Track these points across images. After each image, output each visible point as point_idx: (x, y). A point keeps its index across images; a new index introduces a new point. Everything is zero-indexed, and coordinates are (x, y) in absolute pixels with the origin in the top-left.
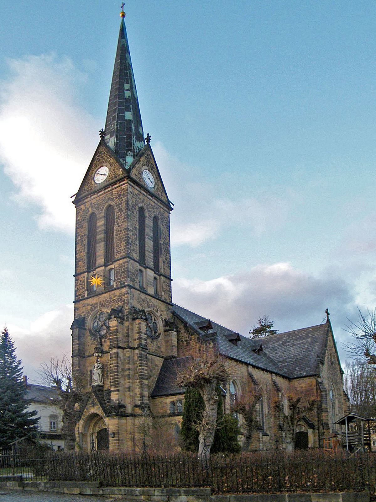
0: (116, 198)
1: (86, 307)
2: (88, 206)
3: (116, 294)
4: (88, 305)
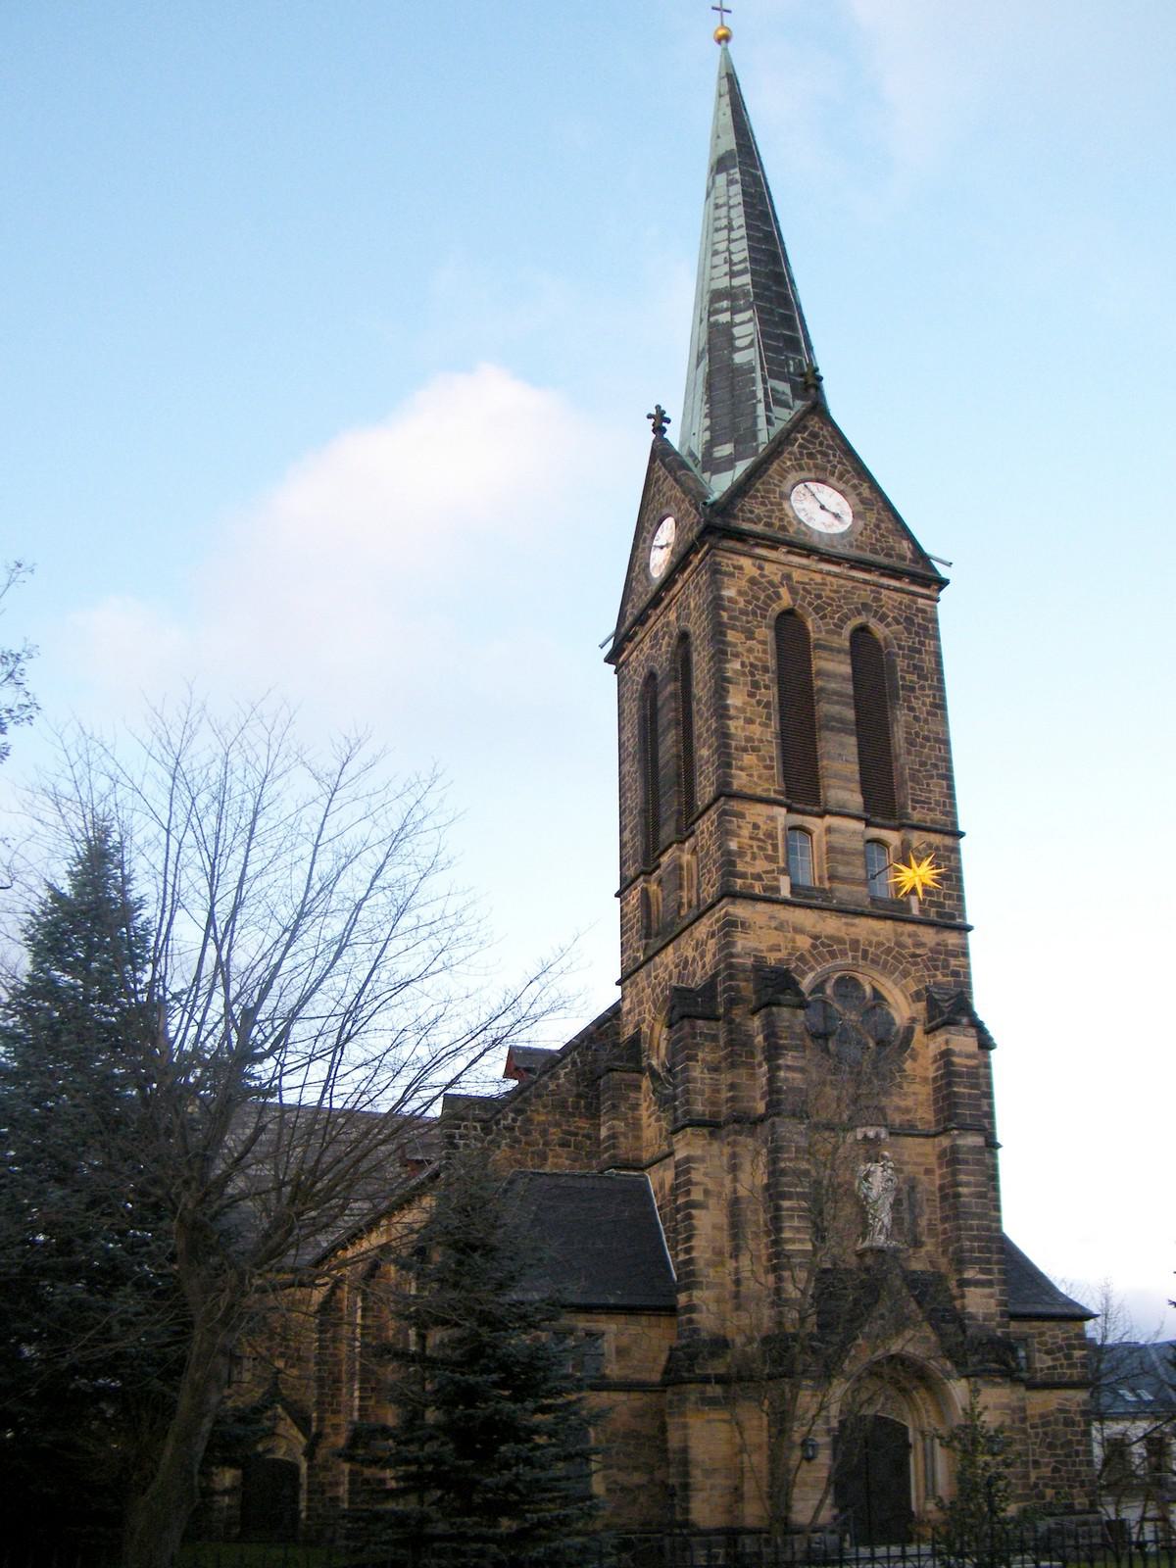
0: (898, 623)
1: (789, 935)
2: (777, 579)
3: (924, 940)
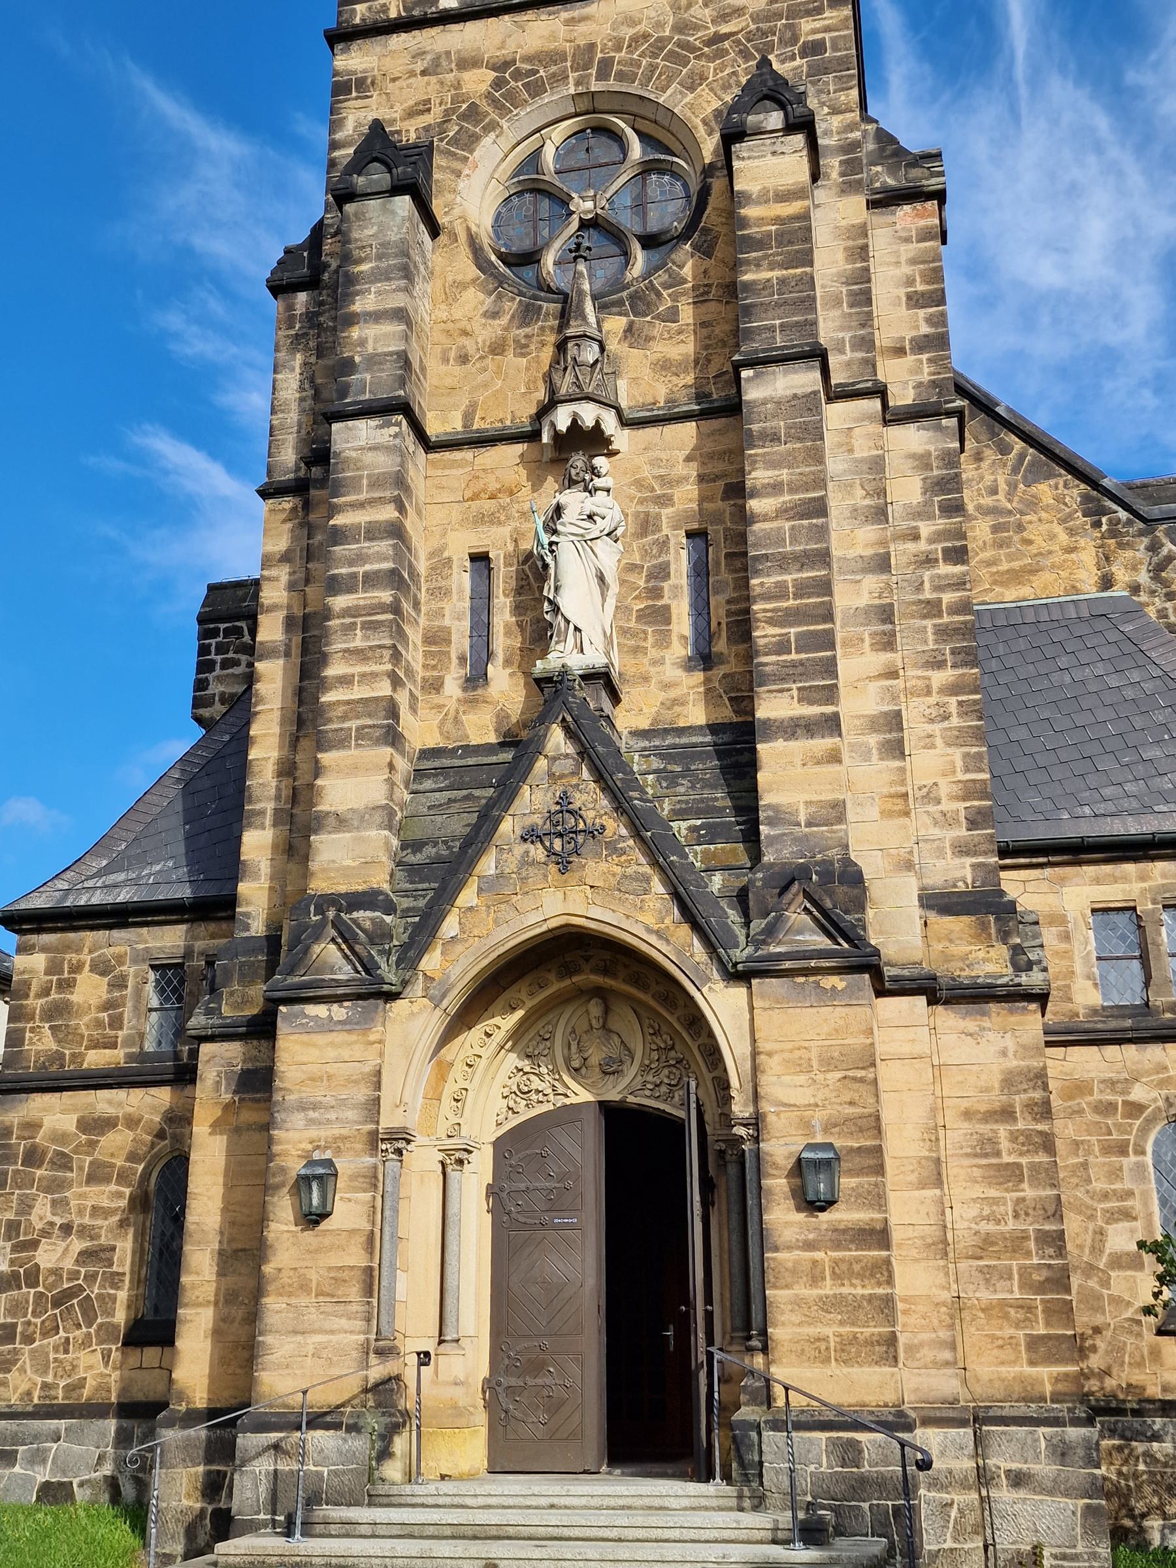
1: (450, 77)
4: (467, 63)
